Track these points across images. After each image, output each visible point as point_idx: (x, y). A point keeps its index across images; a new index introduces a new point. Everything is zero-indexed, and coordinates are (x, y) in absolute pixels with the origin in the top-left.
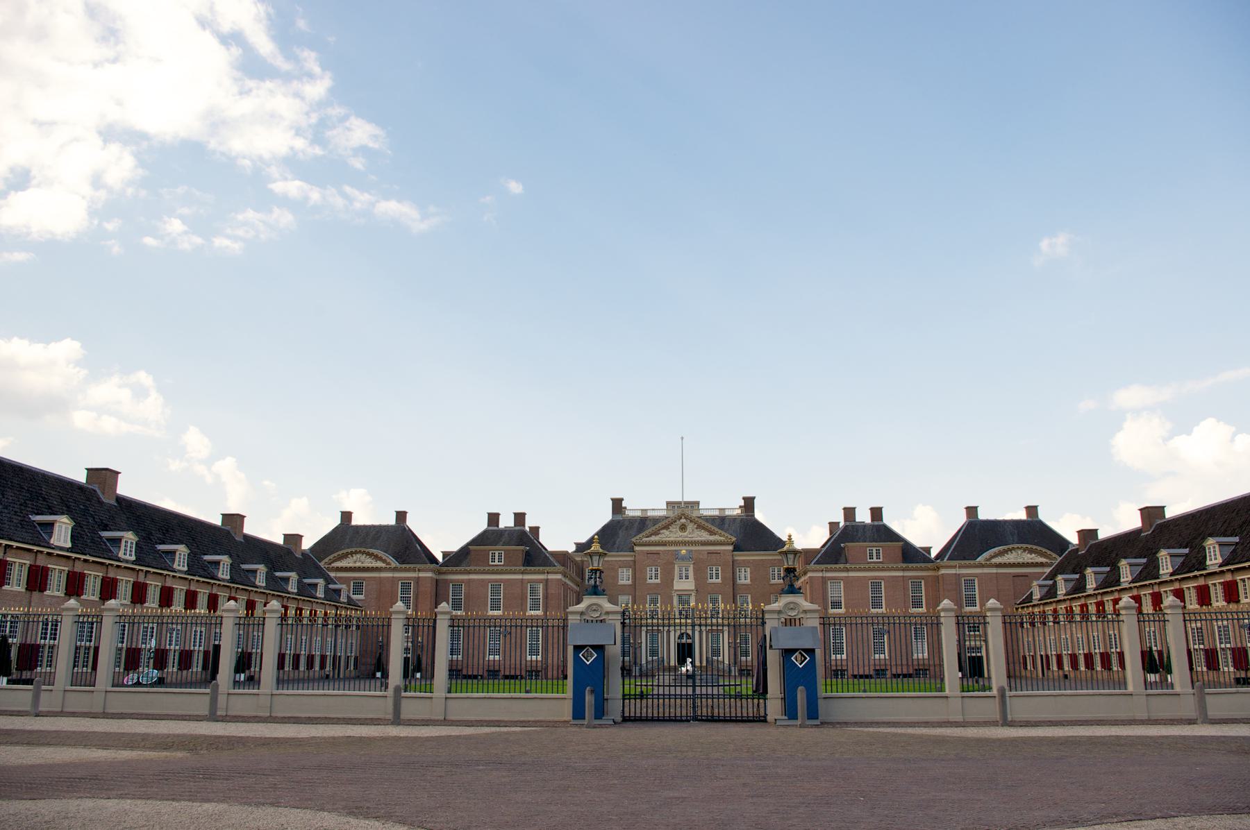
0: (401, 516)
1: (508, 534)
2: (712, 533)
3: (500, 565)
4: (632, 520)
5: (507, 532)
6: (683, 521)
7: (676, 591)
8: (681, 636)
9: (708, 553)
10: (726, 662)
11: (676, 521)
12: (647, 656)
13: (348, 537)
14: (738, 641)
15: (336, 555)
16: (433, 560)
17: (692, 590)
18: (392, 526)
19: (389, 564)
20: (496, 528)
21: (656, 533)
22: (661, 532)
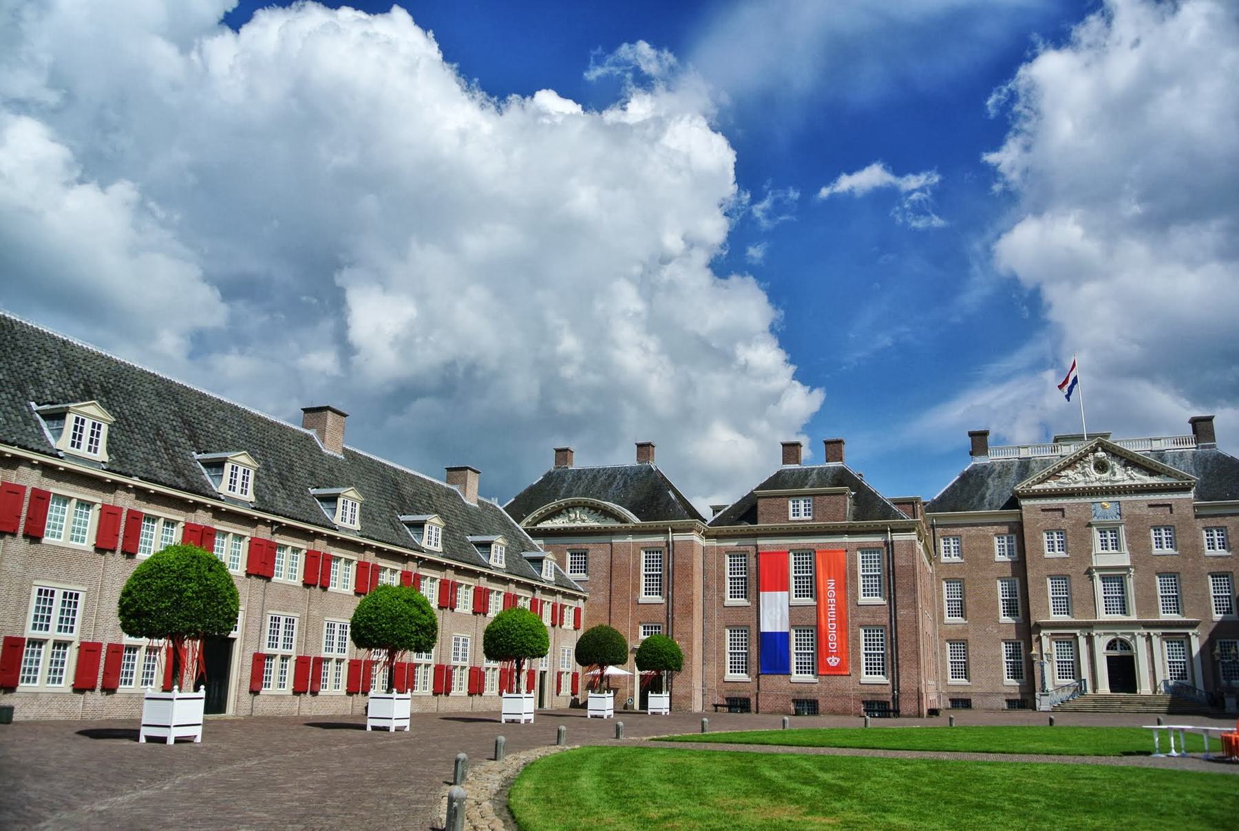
0: (644, 449)
1: (818, 473)
2: (1152, 472)
3: (808, 521)
4: (1006, 467)
5: (815, 472)
6: (1101, 454)
7: (1099, 569)
8: (1111, 646)
9: (1150, 506)
10: (1200, 685)
11: (1087, 456)
12: (1053, 678)
13: (565, 485)
14: (1217, 651)
15: (542, 510)
16: (694, 514)
17: (1126, 568)
18: (631, 468)
19: (624, 521)
20: (797, 466)
21: (1054, 475)
22: (1063, 473)
